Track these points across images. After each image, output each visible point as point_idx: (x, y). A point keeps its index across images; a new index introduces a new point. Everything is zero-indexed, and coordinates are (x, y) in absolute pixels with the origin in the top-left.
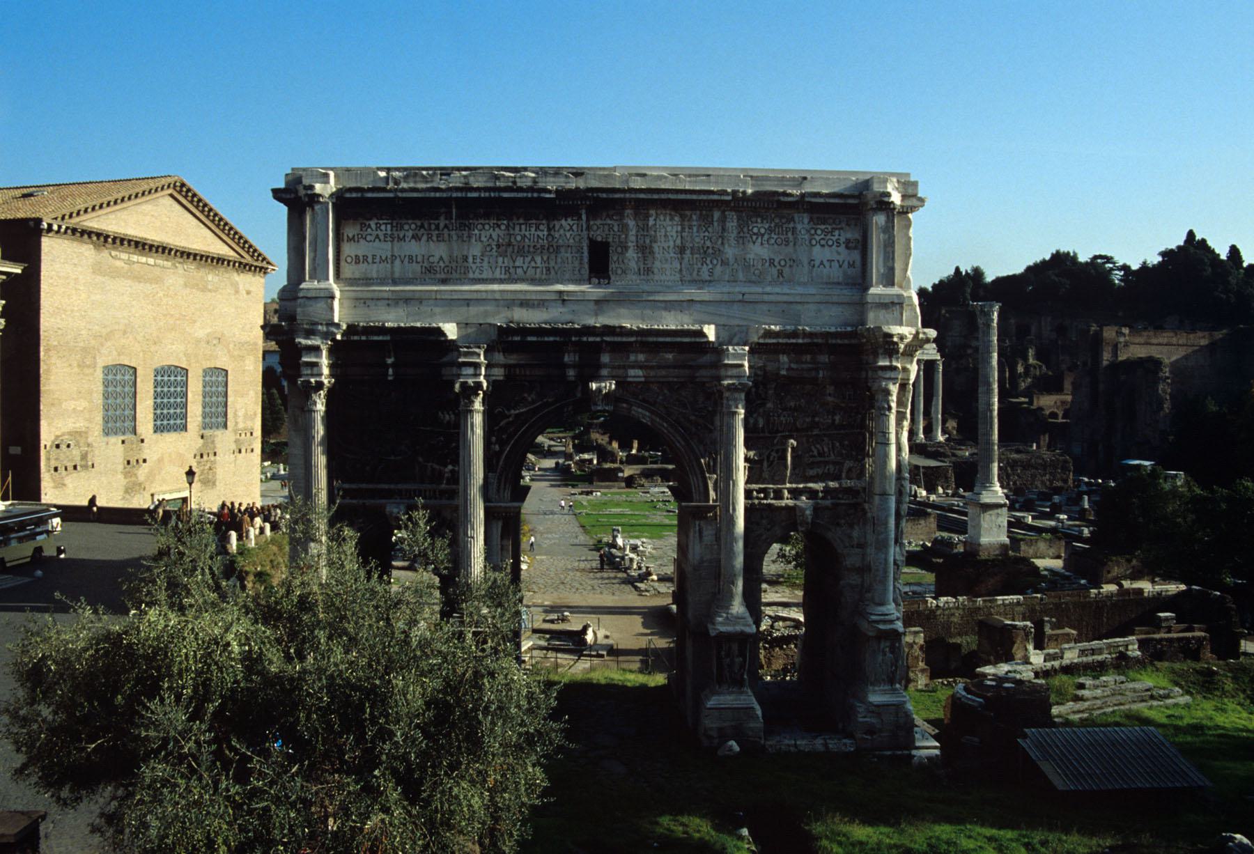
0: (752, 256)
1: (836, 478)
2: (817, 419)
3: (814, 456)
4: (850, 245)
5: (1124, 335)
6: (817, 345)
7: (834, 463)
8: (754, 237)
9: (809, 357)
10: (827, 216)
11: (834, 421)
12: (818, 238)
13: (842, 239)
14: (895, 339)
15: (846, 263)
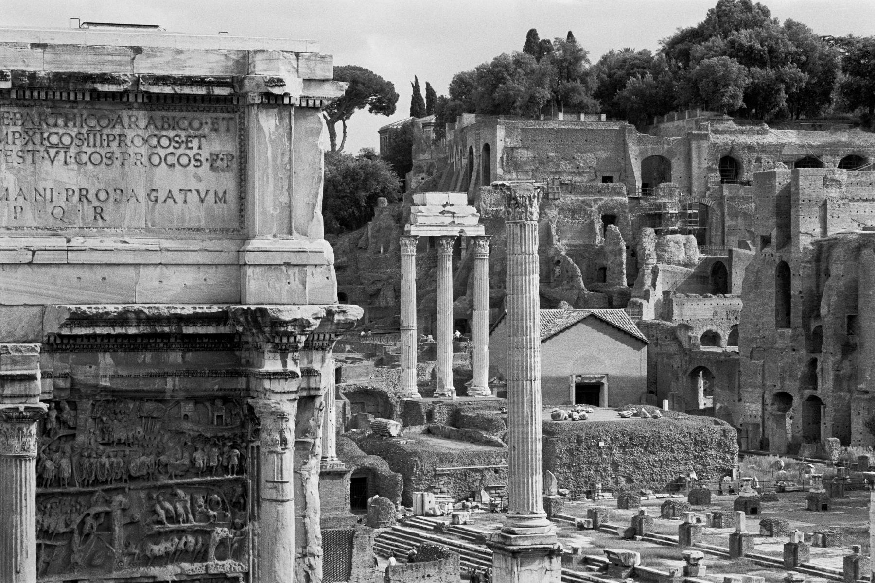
0: (49, 184)
1: (201, 556)
2: (163, 458)
3: (160, 522)
4: (219, 163)
5: (839, 184)
6: (163, 335)
7: (195, 532)
8: (52, 152)
9: (149, 355)
10: (177, 114)
11: (193, 462)
12: (163, 153)
13: (205, 154)
14: (290, 329)
15: (211, 195)
